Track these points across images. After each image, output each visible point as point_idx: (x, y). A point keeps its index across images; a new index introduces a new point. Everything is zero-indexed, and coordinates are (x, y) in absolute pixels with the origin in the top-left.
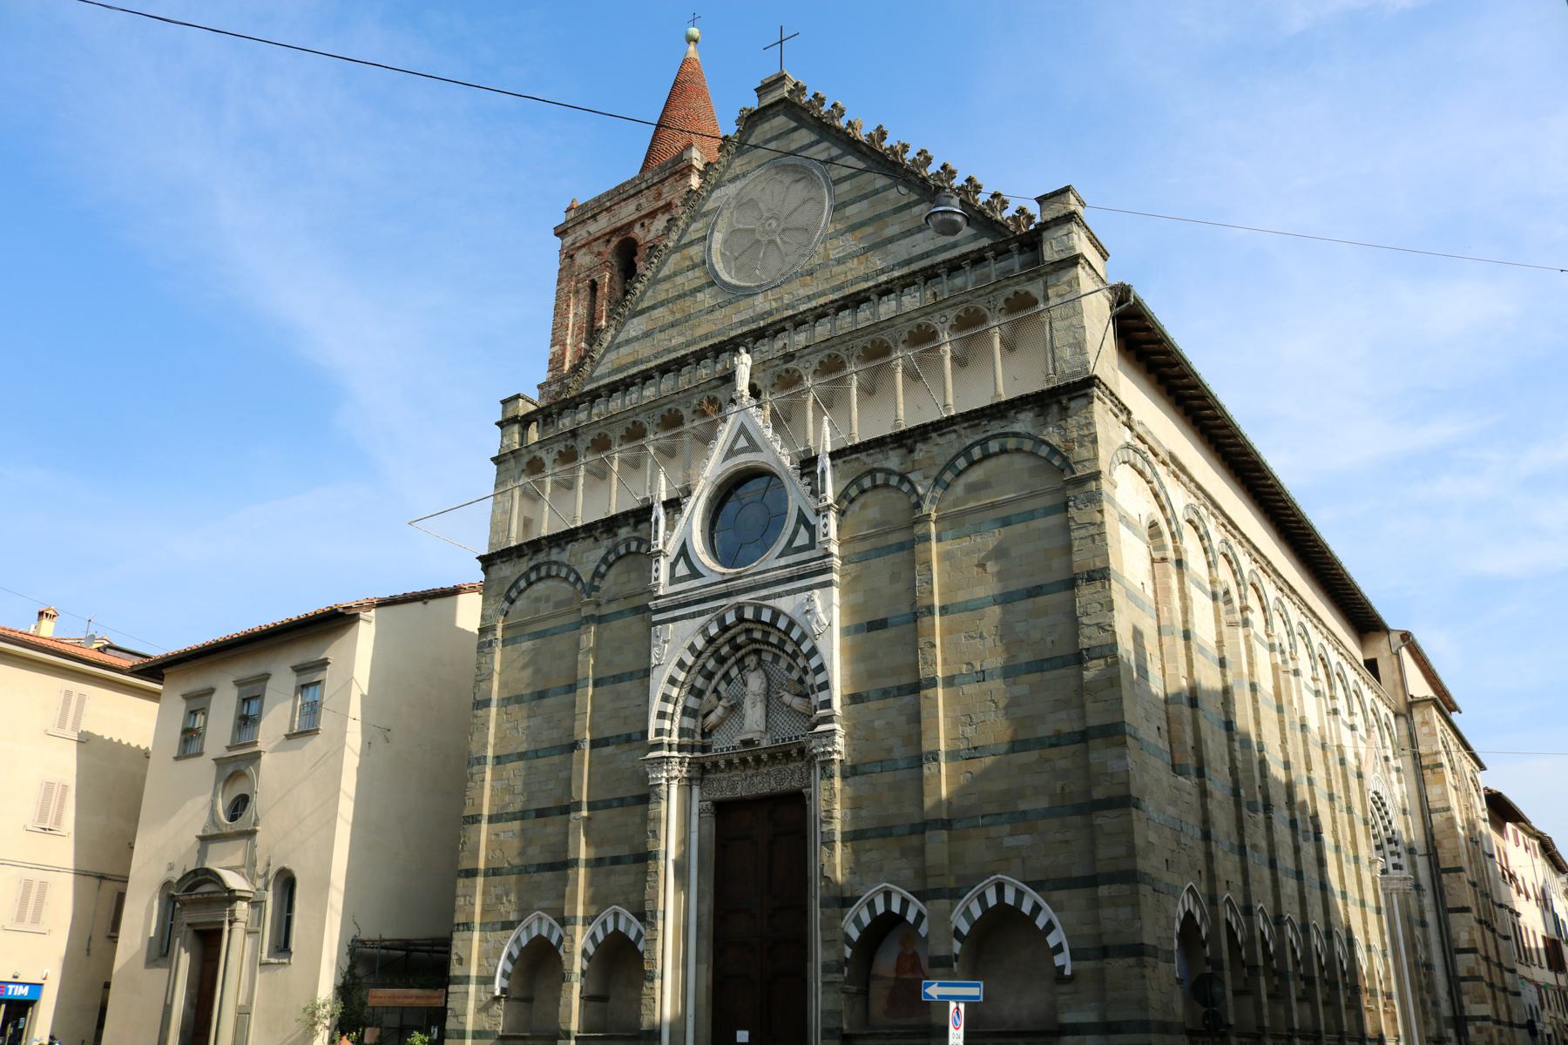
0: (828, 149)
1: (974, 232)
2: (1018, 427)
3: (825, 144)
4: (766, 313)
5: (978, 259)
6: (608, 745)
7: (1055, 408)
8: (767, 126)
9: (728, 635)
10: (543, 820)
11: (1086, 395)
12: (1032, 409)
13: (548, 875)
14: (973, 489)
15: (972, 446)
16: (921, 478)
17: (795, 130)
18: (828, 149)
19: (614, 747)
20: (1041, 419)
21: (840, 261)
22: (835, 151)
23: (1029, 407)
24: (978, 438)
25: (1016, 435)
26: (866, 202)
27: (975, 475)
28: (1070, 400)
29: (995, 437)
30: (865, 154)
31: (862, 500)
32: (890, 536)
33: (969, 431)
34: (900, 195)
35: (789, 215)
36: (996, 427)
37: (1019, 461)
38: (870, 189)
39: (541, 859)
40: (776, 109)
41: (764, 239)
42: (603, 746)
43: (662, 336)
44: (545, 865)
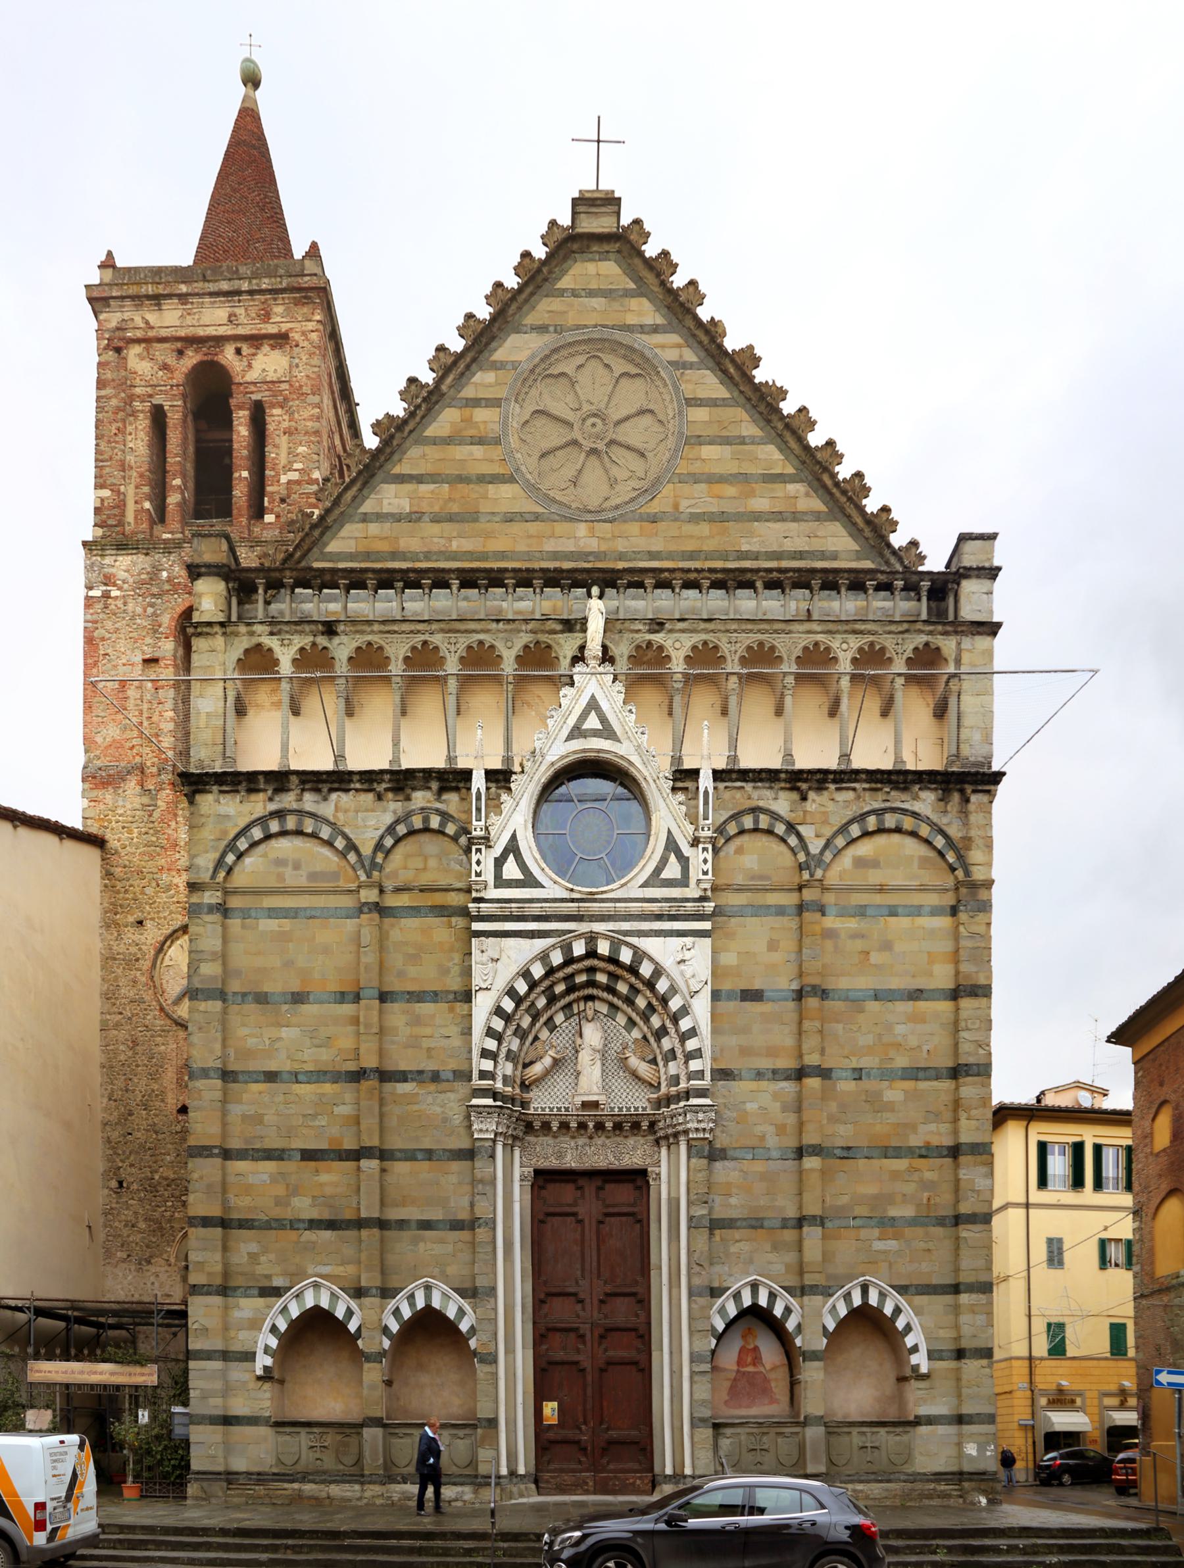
0: (679, 346)
1: (858, 548)
2: (917, 807)
3: (675, 338)
4: (591, 553)
5: (857, 581)
6: (405, 1081)
7: (956, 797)
8: (591, 268)
9: (569, 970)
10: (313, 1164)
11: (988, 792)
12: (936, 789)
13: (327, 1234)
14: (861, 863)
15: (869, 813)
16: (813, 835)
17: (627, 294)
18: (679, 346)
19: (415, 1084)
20: (942, 803)
21: (695, 518)
22: (690, 356)
23: (933, 786)
24: (877, 805)
25: (915, 815)
26: (727, 449)
27: (865, 848)
28: (974, 791)
29: (894, 810)
30: (731, 378)
31: (738, 841)
32: (769, 895)
33: (867, 794)
34: (771, 457)
35: (619, 423)
36: (898, 799)
37: (910, 844)
38: (733, 432)
39: (314, 1214)
40: (606, 247)
41: (587, 444)
42: (399, 1081)
43: (436, 528)
44: (320, 1221)
